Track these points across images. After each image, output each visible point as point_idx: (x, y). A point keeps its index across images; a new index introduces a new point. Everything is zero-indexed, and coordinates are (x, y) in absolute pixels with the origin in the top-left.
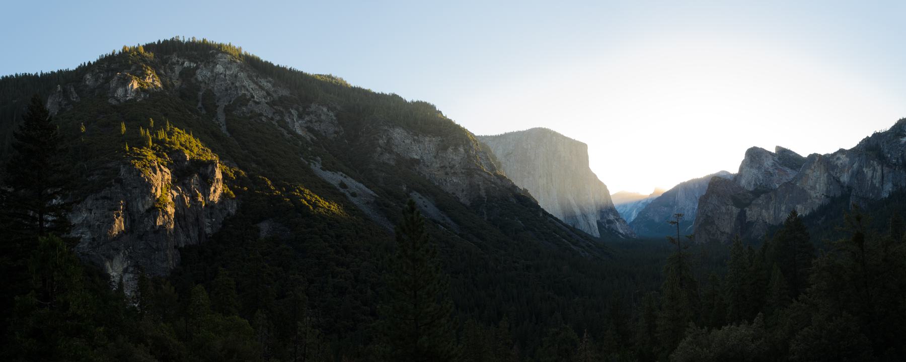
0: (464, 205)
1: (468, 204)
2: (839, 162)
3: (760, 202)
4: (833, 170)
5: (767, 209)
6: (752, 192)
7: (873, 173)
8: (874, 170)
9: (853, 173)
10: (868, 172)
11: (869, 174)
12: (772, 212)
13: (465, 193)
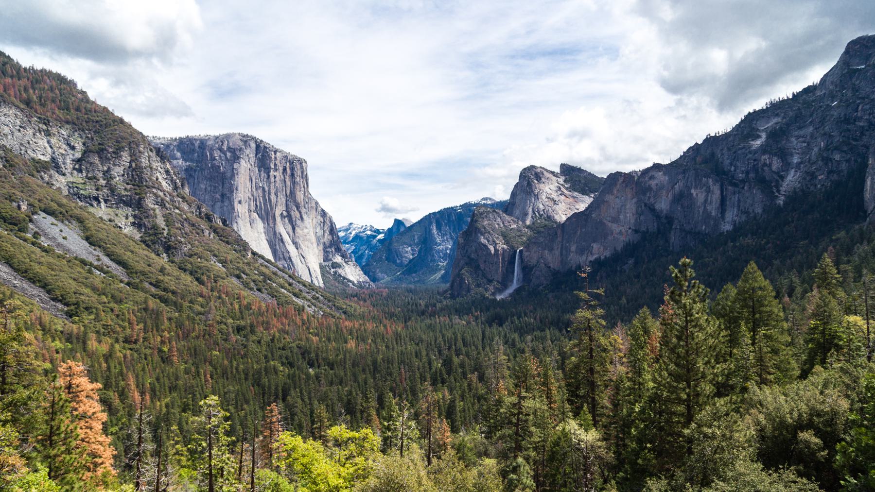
0: (131, 238)
1: (138, 236)
2: (653, 183)
3: (542, 240)
4: (644, 194)
5: (551, 250)
6: (528, 227)
7: (706, 196)
8: (709, 191)
9: (674, 196)
10: (698, 195)
11: (701, 198)
12: (557, 252)
13: (131, 219)
